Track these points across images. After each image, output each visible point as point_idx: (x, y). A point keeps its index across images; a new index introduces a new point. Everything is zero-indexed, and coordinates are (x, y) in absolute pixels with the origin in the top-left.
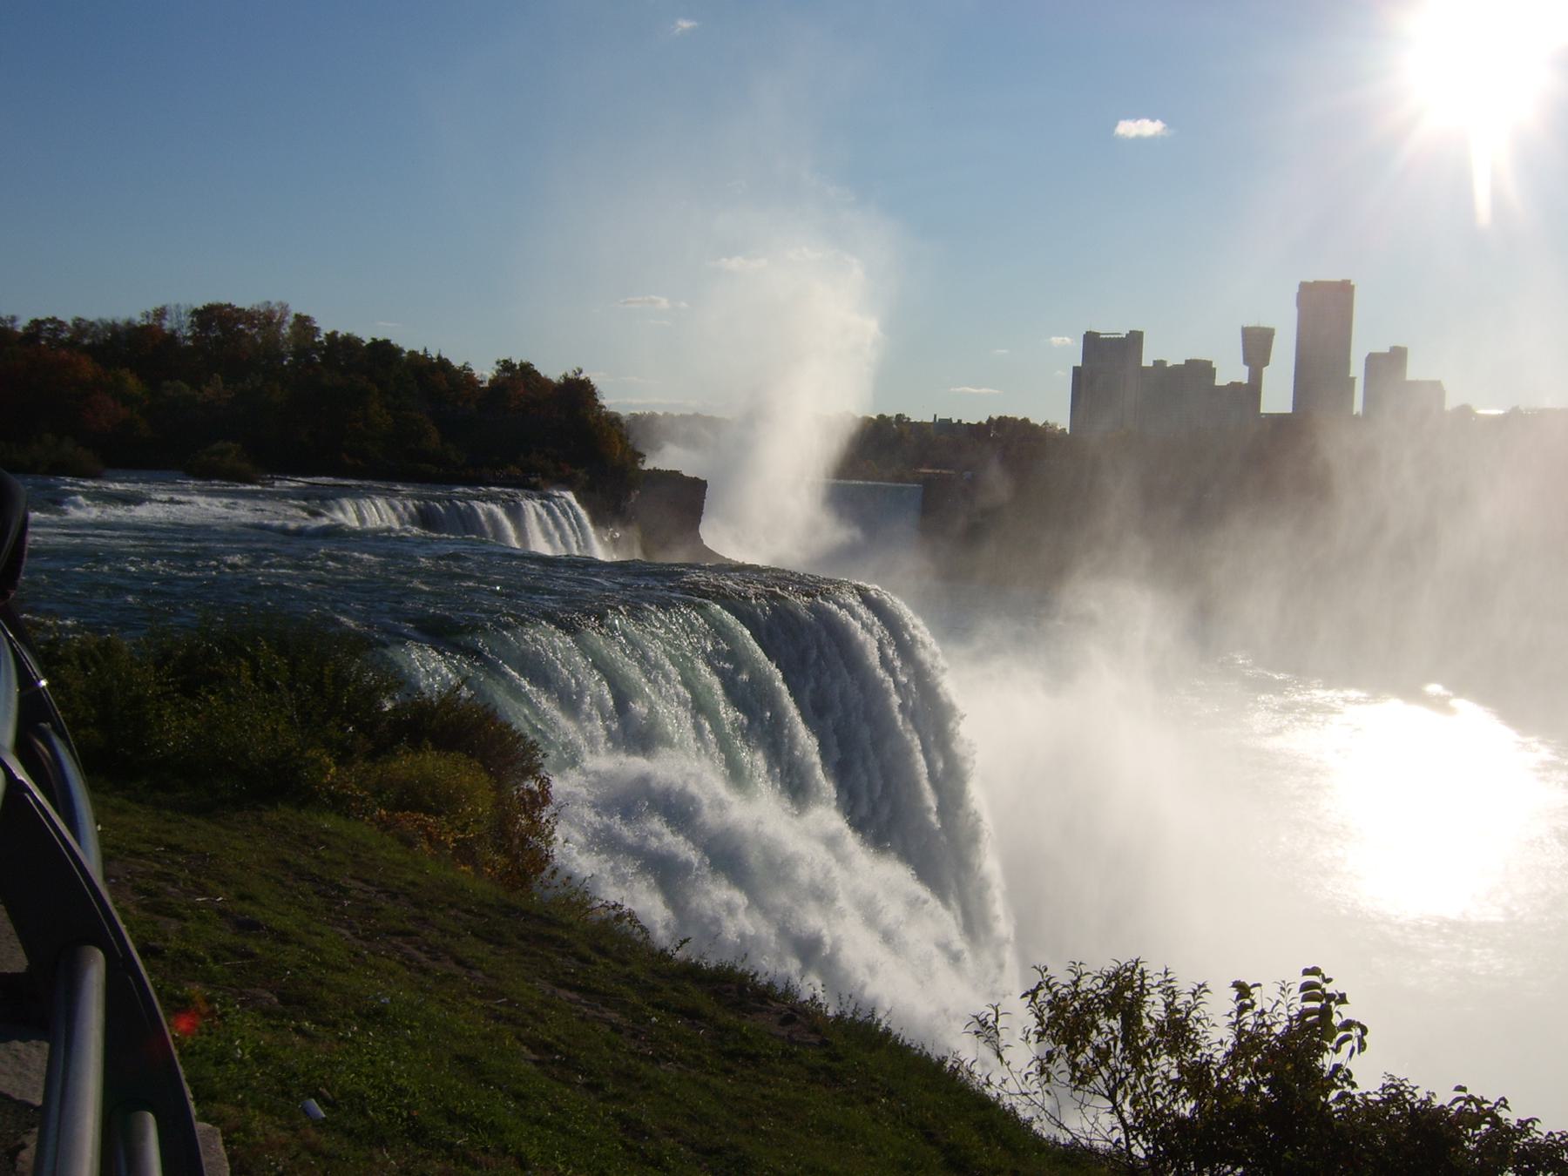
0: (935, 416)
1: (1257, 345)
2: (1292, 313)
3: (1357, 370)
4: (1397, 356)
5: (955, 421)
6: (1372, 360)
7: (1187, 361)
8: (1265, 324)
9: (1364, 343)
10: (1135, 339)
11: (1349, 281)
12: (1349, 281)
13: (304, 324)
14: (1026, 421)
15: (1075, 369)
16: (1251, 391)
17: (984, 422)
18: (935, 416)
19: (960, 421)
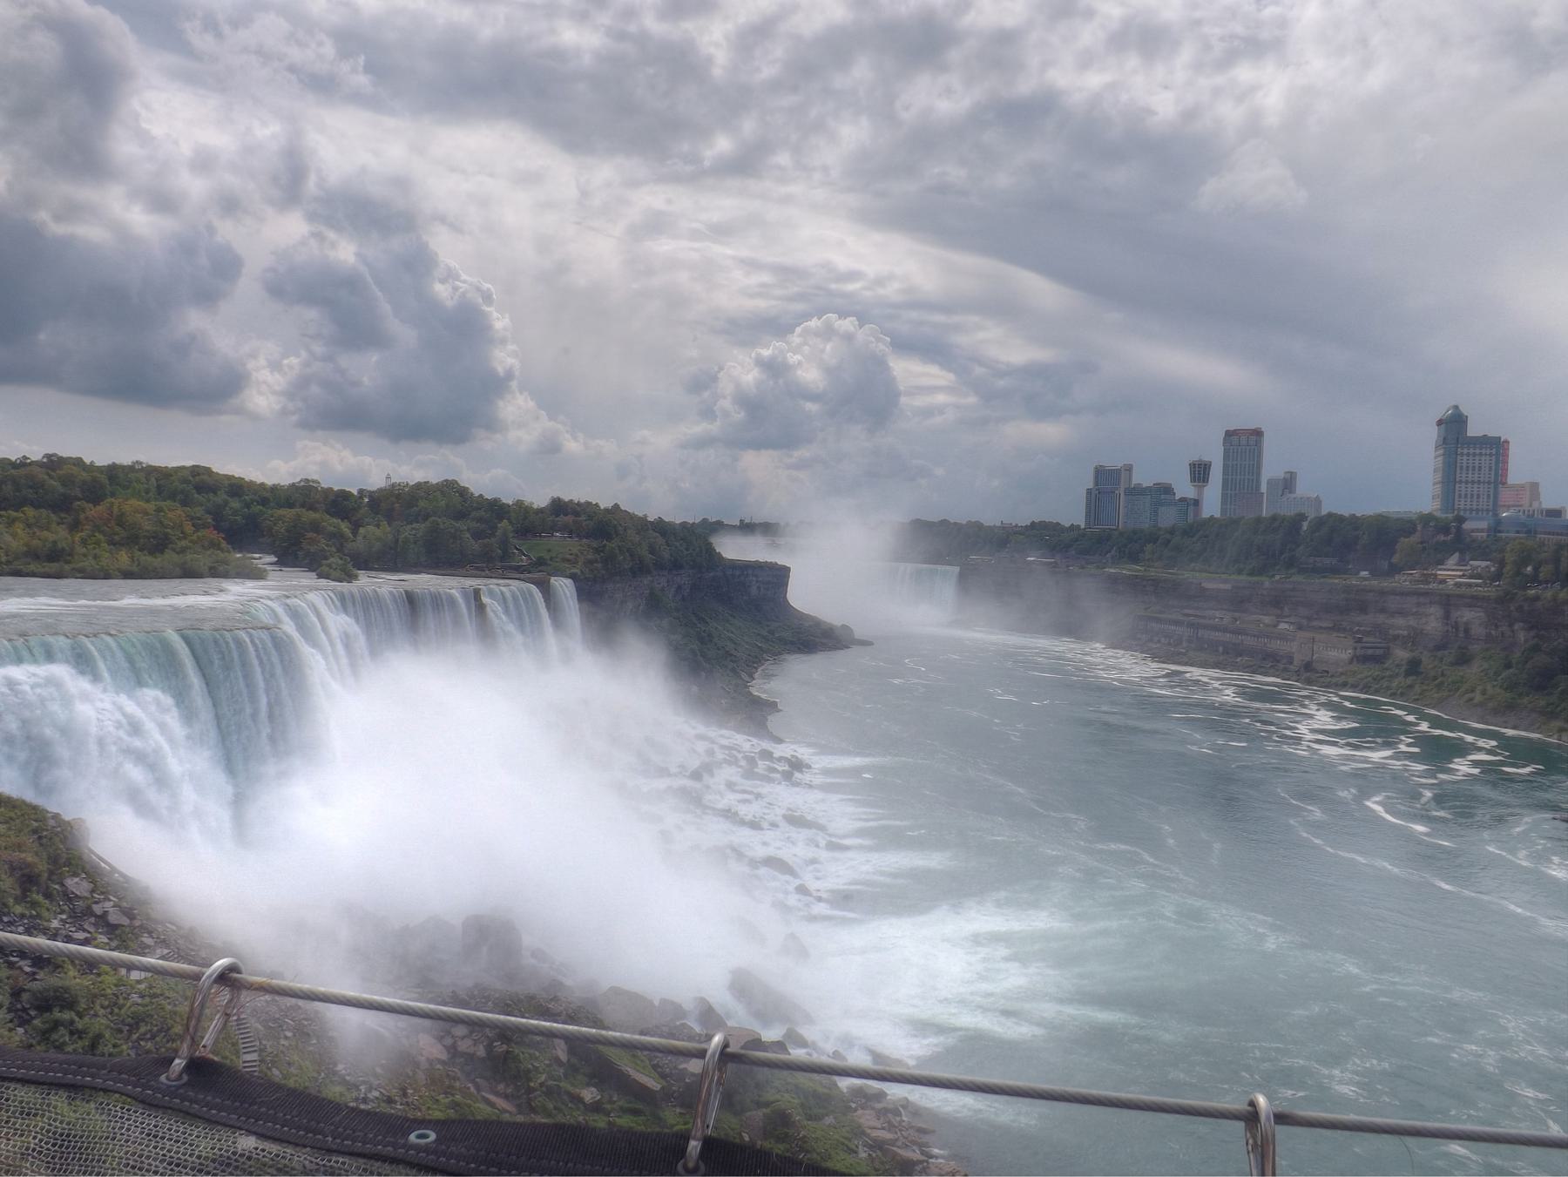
1: (1200, 472)
3: (1264, 488)
5: (1014, 524)
8: (1206, 459)
9: (1272, 467)
10: (1129, 469)
16: (1196, 503)
19: (1016, 526)
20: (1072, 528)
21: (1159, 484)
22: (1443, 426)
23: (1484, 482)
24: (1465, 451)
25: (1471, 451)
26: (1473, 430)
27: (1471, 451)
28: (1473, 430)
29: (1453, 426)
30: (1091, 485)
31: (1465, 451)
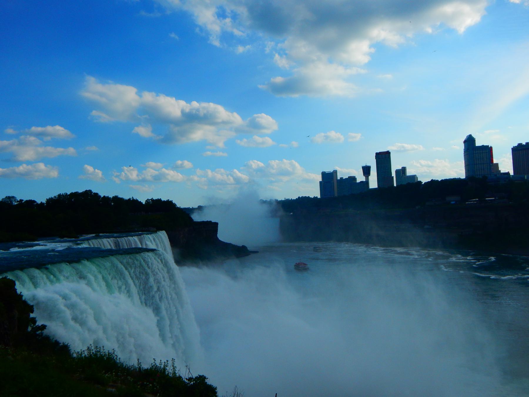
0: (285, 198)
1: (366, 170)
2: (375, 161)
3: (394, 174)
4: (404, 169)
5: (290, 199)
6: (397, 172)
7: (348, 177)
8: (368, 165)
9: (395, 166)
10: (335, 172)
11: (389, 151)
12: (389, 151)
13: (96, 194)
14: (309, 197)
15: (320, 182)
16: (367, 183)
17: (297, 198)
18: (285, 198)
20: (315, 198)
21: (351, 177)
22: (466, 143)
23: (485, 164)
24: (477, 152)
25: (479, 152)
26: (478, 144)
27: (479, 152)
28: (478, 144)
29: (470, 141)
30: (321, 181)
31: (477, 152)
